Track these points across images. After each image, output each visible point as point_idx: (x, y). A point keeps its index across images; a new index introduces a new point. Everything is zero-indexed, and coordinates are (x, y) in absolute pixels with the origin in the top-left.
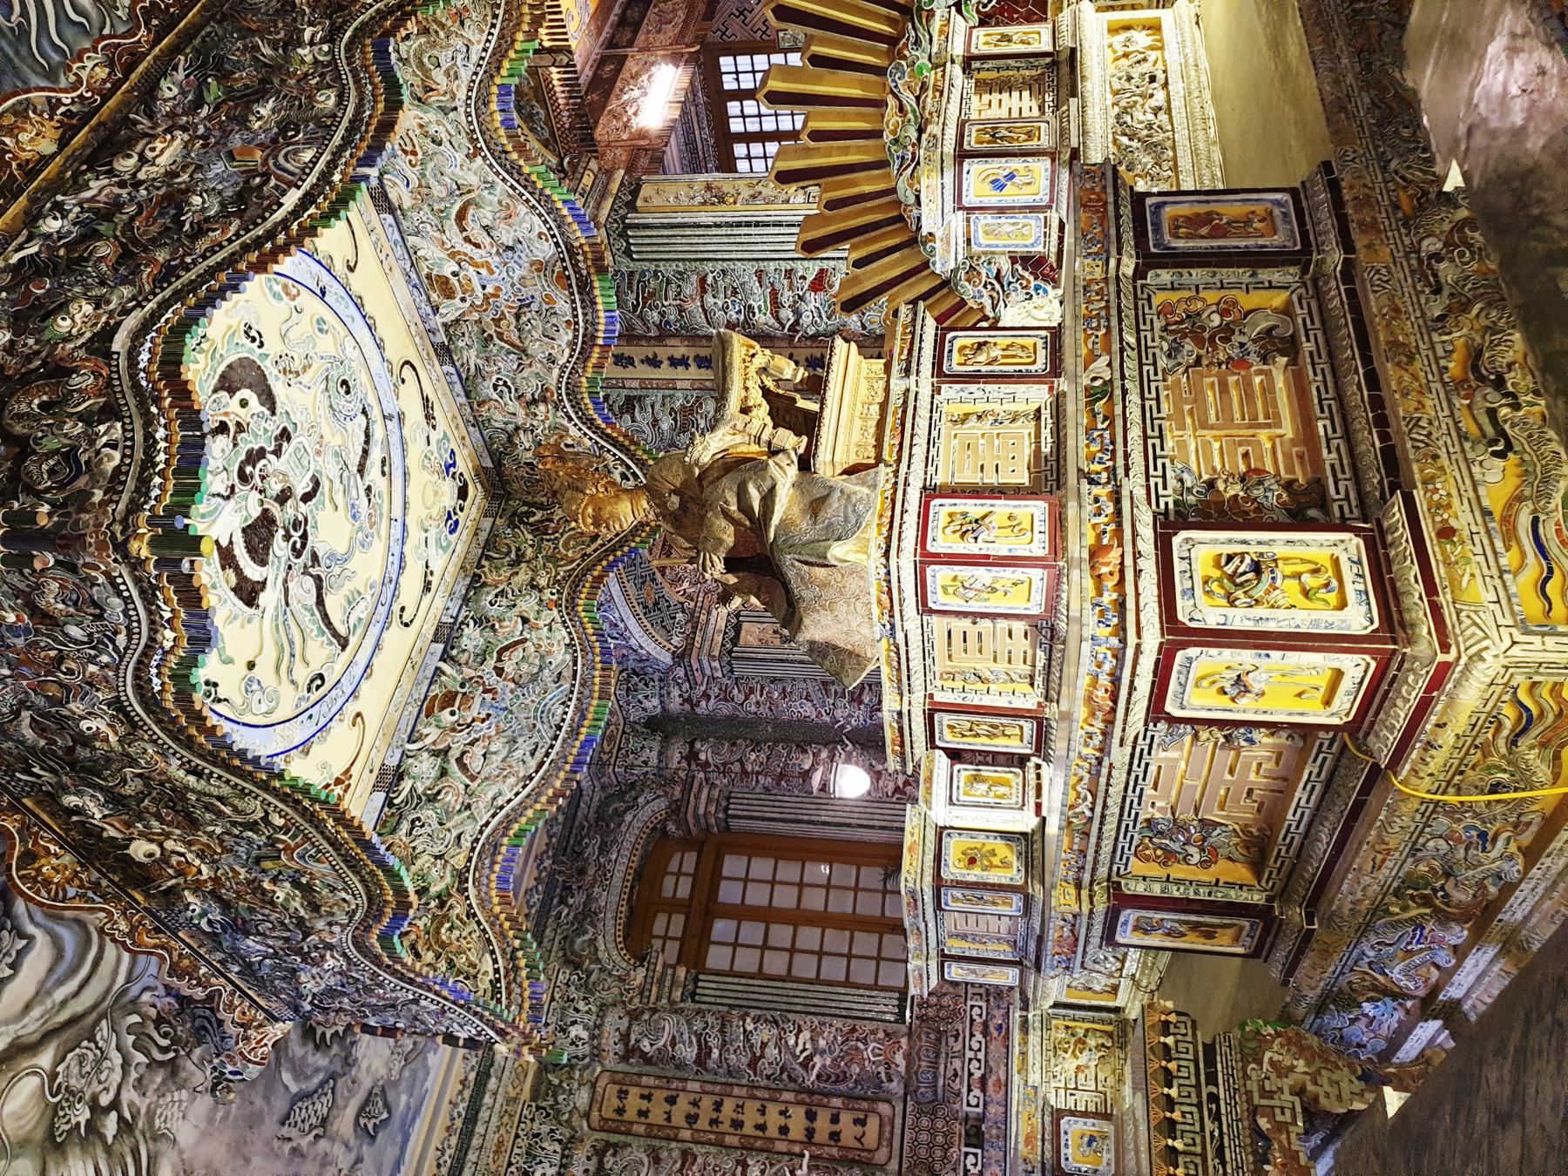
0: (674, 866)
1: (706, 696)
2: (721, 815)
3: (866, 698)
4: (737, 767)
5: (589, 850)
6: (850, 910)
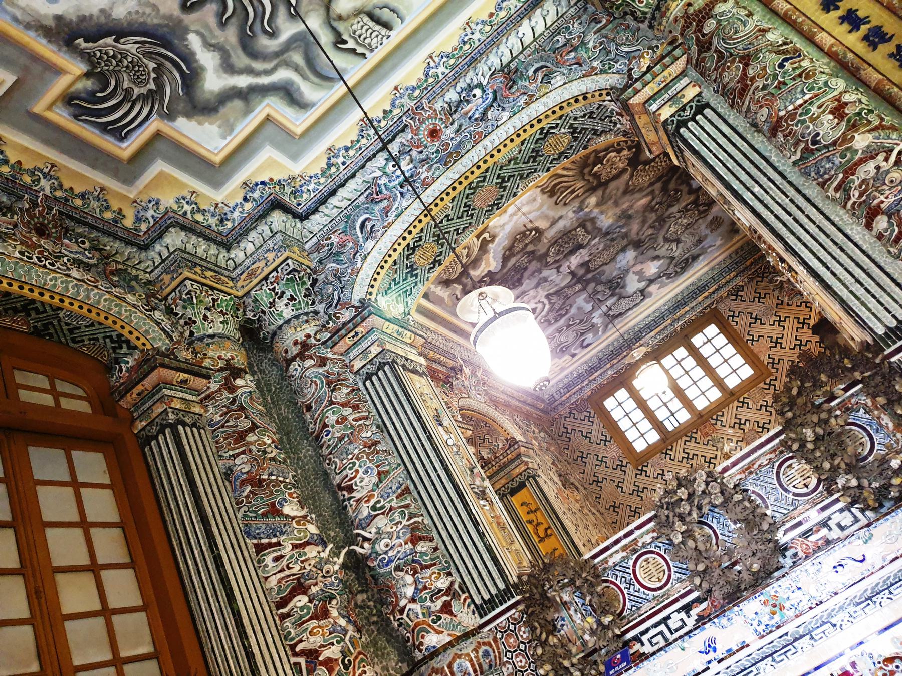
0: (63, 386)
2: (172, 417)
3: (422, 547)
4: (246, 424)
5: (75, 248)
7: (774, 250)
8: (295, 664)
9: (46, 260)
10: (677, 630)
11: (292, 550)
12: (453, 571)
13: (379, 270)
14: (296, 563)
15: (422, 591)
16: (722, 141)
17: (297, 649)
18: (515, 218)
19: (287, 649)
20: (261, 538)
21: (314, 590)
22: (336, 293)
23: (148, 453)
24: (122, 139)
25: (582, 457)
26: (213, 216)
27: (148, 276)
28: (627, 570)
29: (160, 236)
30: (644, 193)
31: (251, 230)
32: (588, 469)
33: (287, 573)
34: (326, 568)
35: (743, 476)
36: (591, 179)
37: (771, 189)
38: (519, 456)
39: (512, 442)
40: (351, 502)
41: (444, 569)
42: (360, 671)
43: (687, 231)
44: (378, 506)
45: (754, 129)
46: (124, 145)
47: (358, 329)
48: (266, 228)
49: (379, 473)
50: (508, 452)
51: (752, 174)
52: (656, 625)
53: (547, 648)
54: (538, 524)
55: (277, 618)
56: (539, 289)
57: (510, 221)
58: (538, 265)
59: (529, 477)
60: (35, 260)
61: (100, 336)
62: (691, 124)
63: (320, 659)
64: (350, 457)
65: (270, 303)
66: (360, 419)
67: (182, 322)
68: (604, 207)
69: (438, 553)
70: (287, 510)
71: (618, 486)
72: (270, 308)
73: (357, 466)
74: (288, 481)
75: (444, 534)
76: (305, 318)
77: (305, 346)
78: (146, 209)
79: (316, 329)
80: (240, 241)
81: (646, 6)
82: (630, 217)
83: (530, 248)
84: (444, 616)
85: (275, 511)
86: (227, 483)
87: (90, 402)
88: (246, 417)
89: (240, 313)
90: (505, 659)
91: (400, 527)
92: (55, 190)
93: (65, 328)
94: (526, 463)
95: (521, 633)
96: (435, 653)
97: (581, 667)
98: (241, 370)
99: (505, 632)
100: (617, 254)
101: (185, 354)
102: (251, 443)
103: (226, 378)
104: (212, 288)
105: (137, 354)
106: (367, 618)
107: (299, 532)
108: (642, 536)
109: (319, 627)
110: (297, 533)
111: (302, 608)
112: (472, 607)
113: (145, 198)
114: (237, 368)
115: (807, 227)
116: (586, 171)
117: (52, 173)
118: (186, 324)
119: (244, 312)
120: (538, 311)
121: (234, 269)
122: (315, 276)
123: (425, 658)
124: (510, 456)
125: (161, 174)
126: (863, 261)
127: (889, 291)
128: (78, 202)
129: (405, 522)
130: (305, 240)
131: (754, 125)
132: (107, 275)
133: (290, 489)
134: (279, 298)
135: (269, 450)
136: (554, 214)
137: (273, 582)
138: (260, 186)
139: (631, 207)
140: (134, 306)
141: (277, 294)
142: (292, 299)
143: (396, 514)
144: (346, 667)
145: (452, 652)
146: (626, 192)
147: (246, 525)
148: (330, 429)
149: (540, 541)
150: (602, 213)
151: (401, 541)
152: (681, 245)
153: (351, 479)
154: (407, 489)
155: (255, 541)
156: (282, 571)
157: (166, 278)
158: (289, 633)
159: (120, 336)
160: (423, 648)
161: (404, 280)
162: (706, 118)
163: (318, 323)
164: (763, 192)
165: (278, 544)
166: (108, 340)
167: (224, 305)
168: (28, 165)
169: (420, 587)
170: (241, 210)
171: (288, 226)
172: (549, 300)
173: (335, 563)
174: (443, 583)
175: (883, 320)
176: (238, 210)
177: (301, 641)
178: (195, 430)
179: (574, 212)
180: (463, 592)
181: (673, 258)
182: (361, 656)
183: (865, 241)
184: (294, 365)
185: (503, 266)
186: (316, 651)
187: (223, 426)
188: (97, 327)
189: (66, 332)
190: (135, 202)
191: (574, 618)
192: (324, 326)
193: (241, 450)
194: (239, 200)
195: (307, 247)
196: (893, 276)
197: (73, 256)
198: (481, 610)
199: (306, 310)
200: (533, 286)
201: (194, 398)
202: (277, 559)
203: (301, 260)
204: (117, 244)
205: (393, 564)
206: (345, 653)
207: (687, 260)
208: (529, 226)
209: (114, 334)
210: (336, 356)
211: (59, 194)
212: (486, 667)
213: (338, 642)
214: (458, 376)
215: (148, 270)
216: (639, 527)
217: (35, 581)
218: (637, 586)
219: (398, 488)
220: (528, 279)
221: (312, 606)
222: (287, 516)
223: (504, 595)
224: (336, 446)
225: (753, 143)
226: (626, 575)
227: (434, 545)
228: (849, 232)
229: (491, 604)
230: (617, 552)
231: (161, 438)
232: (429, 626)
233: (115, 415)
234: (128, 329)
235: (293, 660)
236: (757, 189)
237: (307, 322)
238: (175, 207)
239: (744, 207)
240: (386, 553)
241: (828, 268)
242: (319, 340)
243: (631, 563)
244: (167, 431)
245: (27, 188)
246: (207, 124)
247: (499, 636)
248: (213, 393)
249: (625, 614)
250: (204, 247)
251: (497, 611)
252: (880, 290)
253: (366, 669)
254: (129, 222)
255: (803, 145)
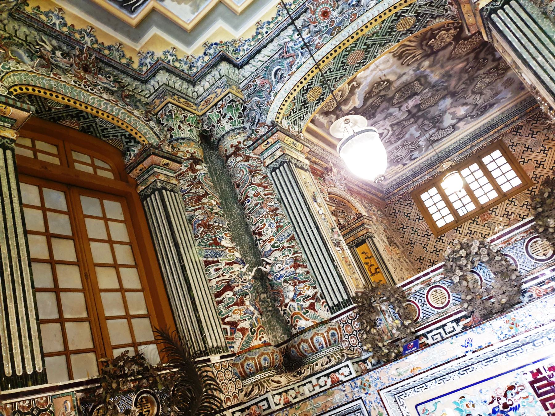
0: (98, 163)
1: (247, 159)
2: (159, 185)
3: (300, 270)
4: (201, 192)
5: (105, 80)
6: (107, 314)
7: (546, 101)
8: (224, 329)
9: (89, 87)
10: (449, 333)
11: (225, 265)
12: (317, 286)
13: (284, 103)
14: (227, 273)
15: (298, 295)
16: (520, 23)
17: (226, 321)
18: (374, 73)
19: (220, 320)
20: (208, 258)
21: (236, 289)
22: (257, 117)
23: (145, 205)
24: (132, 12)
25: (403, 228)
26: (186, 64)
27: (146, 99)
28: (423, 296)
29: (154, 75)
30: (462, 60)
31: (208, 74)
32: (406, 235)
33: (222, 278)
34: (244, 277)
35: (503, 245)
36: (427, 49)
37: (550, 59)
38: (363, 224)
39: (359, 216)
40: (260, 241)
41: (312, 284)
42: (260, 336)
43: (488, 87)
44: (276, 245)
45: (544, 16)
46: (133, 16)
47: (270, 140)
48: (217, 73)
49: (277, 227)
50: (357, 221)
51: (539, 48)
52: (437, 329)
53: (370, 335)
54: (371, 265)
55: (215, 303)
56: (386, 121)
57: (371, 74)
58: (387, 104)
59: (368, 237)
60: (83, 86)
61: (119, 134)
62: (500, 12)
63: (238, 327)
64: (261, 216)
65: (218, 121)
66: (268, 195)
67: (166, 129)
68: (434, 68)
69: (309, 275)
70: (223, 243)
71: (424, 247)
72: (218, 123)
73: (264, 222)
74: (225, 226)
75: (313, 264)
76: (238, 131)
77: (237, 148)
78: (146, 58)
79: (244, 138)
80: (201, 80)
82: (450, 76)
83: (383, 93)
84: (310, 311)
85: (216, 243)
86: (190, 225)
87: (113, 173)
88: (202, 188)
89: (200, 125)
90: (344, 339)
91: (288, 258)
92: (93, 43)
93: (99, 128)
94: (367, 229)
95: (355, 325)
96: (304, 331)
97: (389, 347)
98: (200, 160)
99: (346, 323)
100: (439, 100)
101: (167, 148)
102: (205, 204)
103: (191, 164)
104: (184, 109)
105: (140, 146)
106: (266, 308)
107: (230, 256)
108: (434, 276)
109: (238, 310)
110: (229, 256)
111: (229, 299)
112: (327, 307)
113: (146, 51)
114: (197, 159)
116: (424, 43)
117: (92, 33)
118: (168, 130)
119: (202, 125)
120: (384, 135)
121: (197, 98)
122: (245, 105)
123: (298, 333)
124: (357, 224)
125: (155, 37)
128: (106, 52)
129: (291, 256)
130: (240, 82)
131: (545, 13)
132: (123, 98)
133: (226, 231)
134: (223, 118)
135: (214, 208)
136: (400, 71)
137: (214, 282)
138: (214, 46)
139: (452, 69)
140: (138, 118)
141: (222, 115)
142: (230, 118)
143: (286, 251)
144: (253, 333)
145: (313, 331)
146: (449, 59)
147: (200, 250)
148: (250, 199)
149: (371, 275)
150: (432, 72)
151: (288, 266)
152: (483, 97)
153: (261, 229)
154: (293, 238)
155: (205, 259)
156: (219, 277)
157: (157, 101)
158: (222, 311)
159: (130, 135)
160: (297, 327)
161: (299, 110)
162: (511, 7)
163: (245, 135)
164: (544, 61)
165: (218, 262)
166: (123, 137)
167: (191, 120)
168: (77, 28)
169: (298, 293)
170: (202, 61)
171: (230, 72)
172: (392, 128)
173: (249, 275)
174: (311, 292)
176: (201, 60)
177: (228, 317)
178: (172, 193)
179: (413, 70)
180: (323, 299)
181: (476, 105)
182: (261, 328)
184: (231, 159)
185: (364, 104)
186: (236, 323)
187: (188, 192)
188: (117, 129)
189: (100, 131)
190: (139, 53)
191: (388, 320)
192: (249, 137)
193: (198, 207)
194: (201, 54)
195: (241, 86)
197: (103, 85)
198: (332, 310)
199: (239, 126)
200: (382, 118)
201: (172, 175)
202: (217, 270)
203: (237, 94)
204: (129, 79)
205: (283, 279)
206: (252, 326)
207: (486, 106)
208: (383, 78)
209: (127, 134)
210: (255, 156)
211: (96, 46)
212: (332, 342)
213: (249, 319)
214: (329, 173)
215: (147, 96)
216: (433, 271)
217: (85, 269)
218: (428, 305)
219: (288, 236)
220: (380, 113)
221: (235, 297)
222: (223, 246)
223: (346, 303)
224: (253, 209)
225: (542, 26)
226: (422, 298)
227: (307, 270)
229: (338, 306)
230: (418, 284)
231: (153, 196)
232: (301, 315)
233: (127, 181)
234: (134, 131)
235: (223, 326)
236: (540, 59)
237: (239, 133)
238: (163, 57)
239: (529, 71)
240: (279, 272)
242: (245, 145)
243: (426, 291)
244: (156, 193)
245: (78, 42)
246: (183, 4)
247: (342, 325)
248: (183, 172)
249: (418, 320)
250: (179, 83)
251: (342, 311)
253: (264, 335)
254: (136, 66)
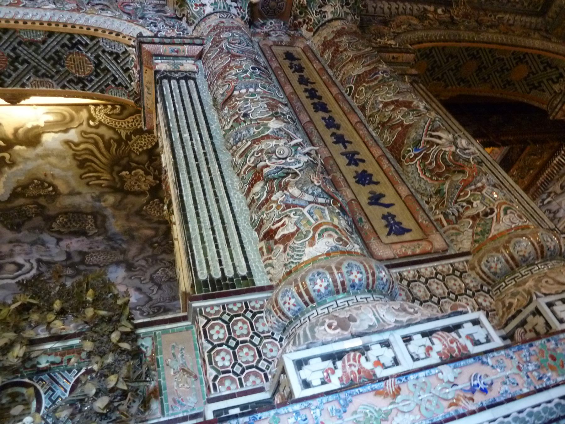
18: (40, 161)
30: (151, 226)
36: (117, 179)
43: (168, 283)
56: (34, 248)
57: (35, 160)
58: (43, 224)
68: (117, 213)
81: (197, 12)
82: (133, 238)
83: (42, 201)
100: (112, 263)
115: (203, 174)
116: (117, 168)
120: (24, 269)
126: (227, 217)
127: (232, 247)
136: (74, 183)
139: (137, 229)
146: (139, 213)
150: (114, 216)
152: (160, 292)
164: (189, 138)
172: (39, 266)
175: (212, 268)
179: (92, 197)
181: (150, 299)
183: (239, 206)
185: (10, 200)
196: (243, 239)
200: (29, 240)
207: (160, 307)
208: (50, 179)
220: (29, 230)
228: (231, 194)
236: (186, 136)
241: (196, 208)
252: (225, 242)
255: (237, 116)
